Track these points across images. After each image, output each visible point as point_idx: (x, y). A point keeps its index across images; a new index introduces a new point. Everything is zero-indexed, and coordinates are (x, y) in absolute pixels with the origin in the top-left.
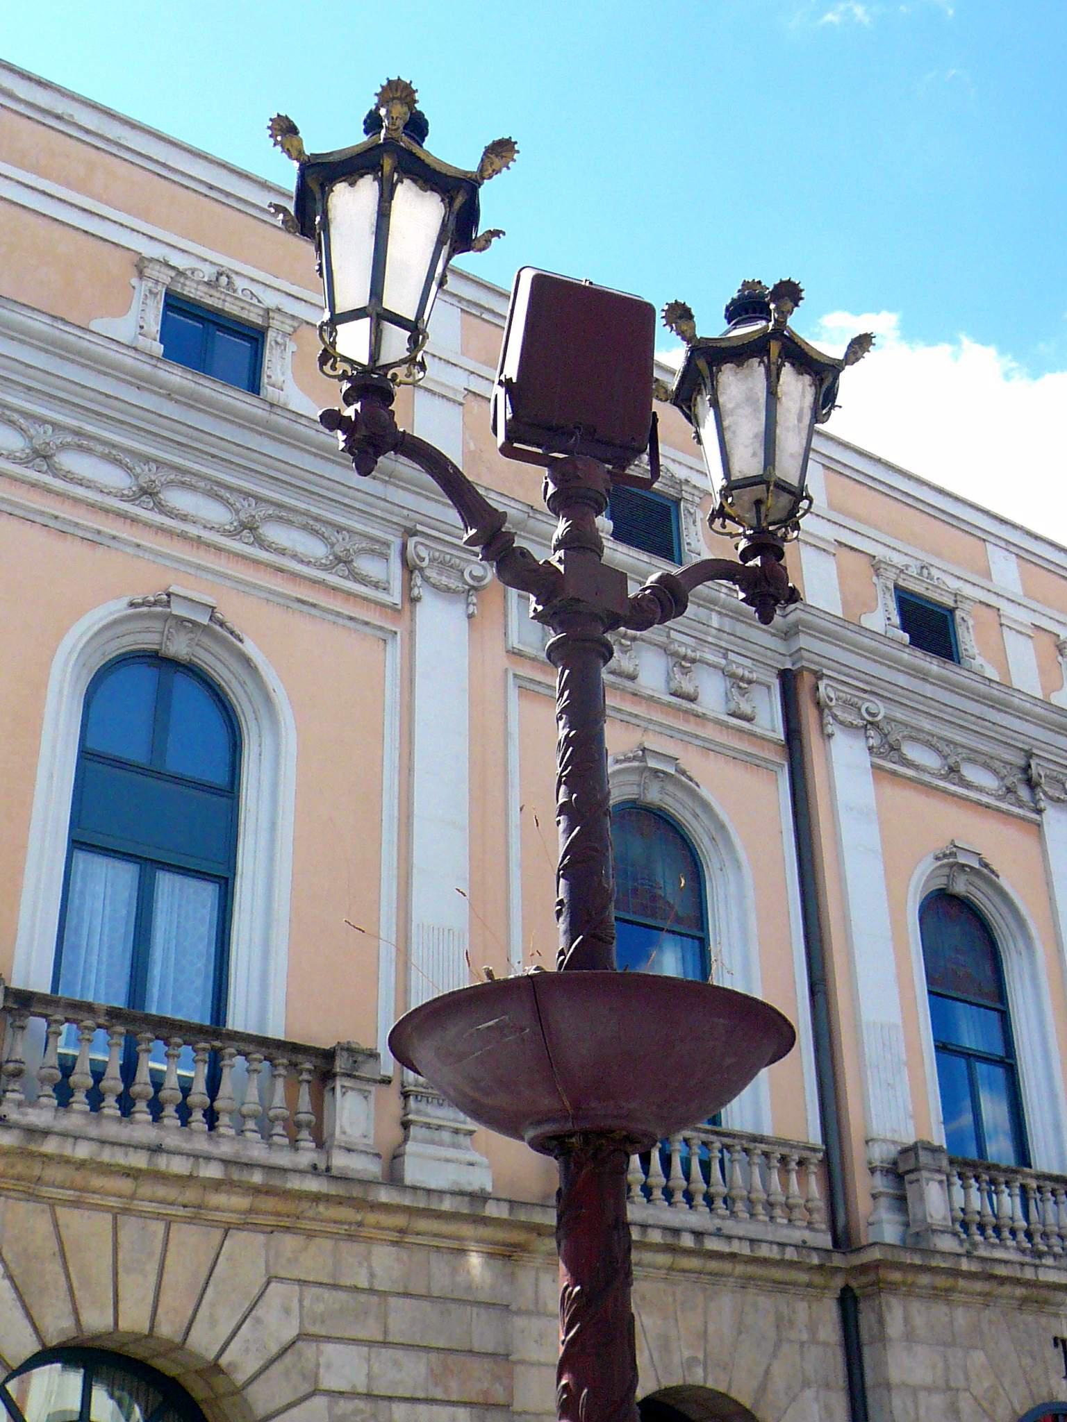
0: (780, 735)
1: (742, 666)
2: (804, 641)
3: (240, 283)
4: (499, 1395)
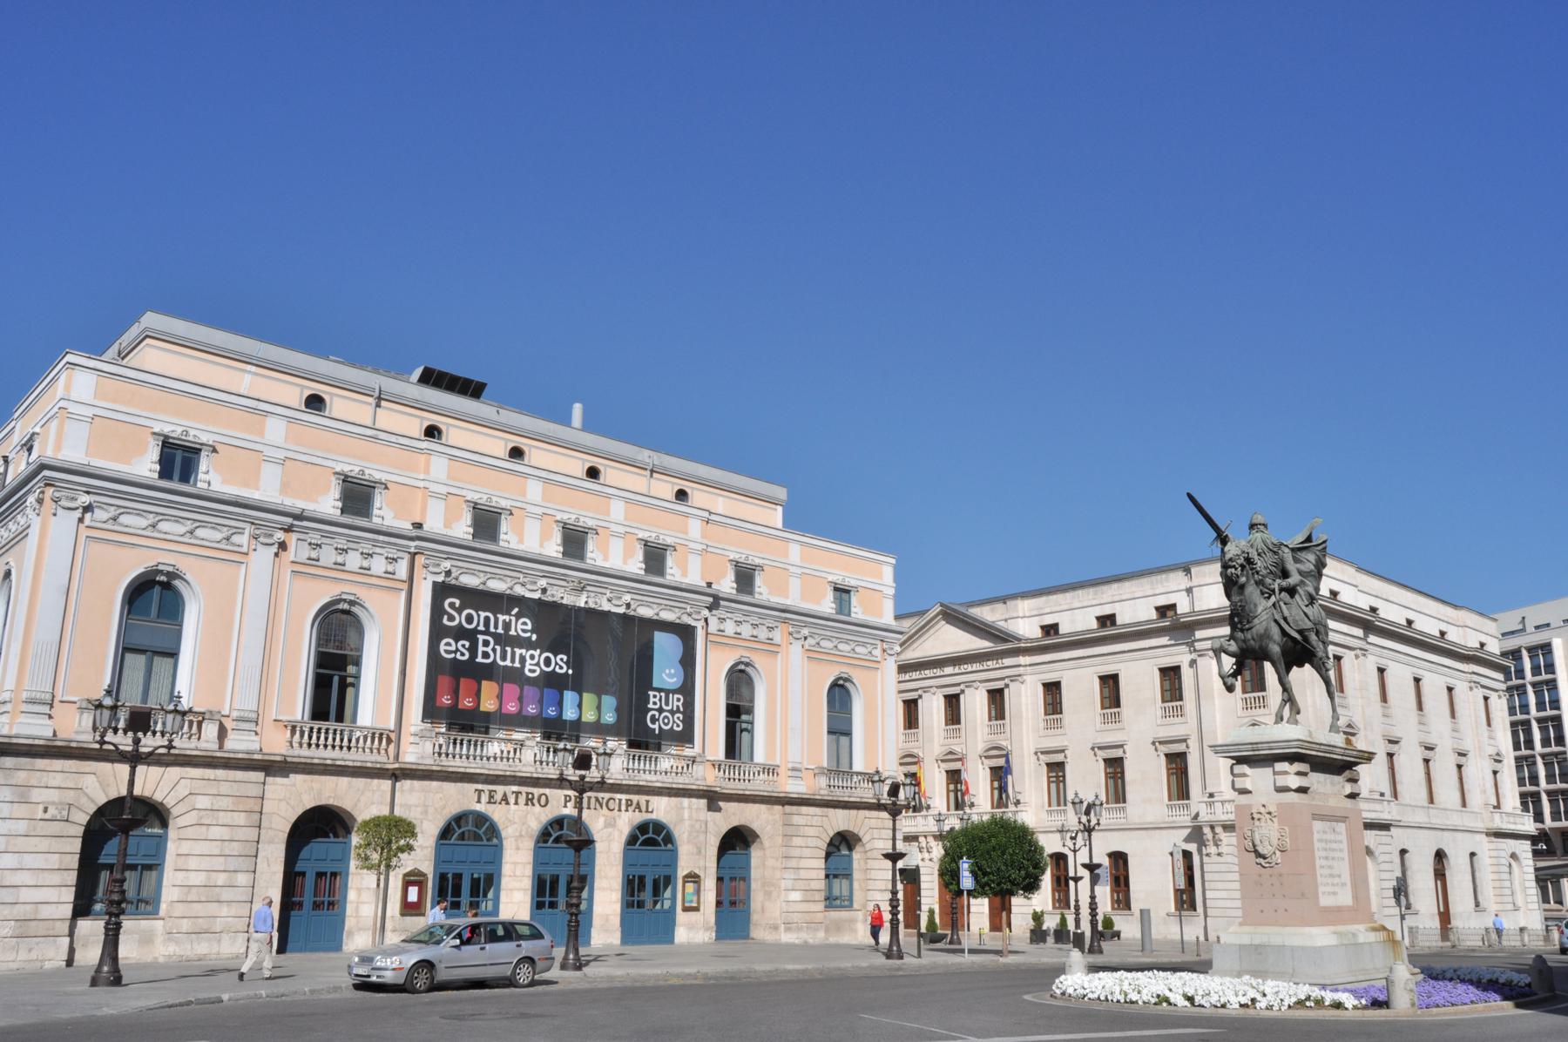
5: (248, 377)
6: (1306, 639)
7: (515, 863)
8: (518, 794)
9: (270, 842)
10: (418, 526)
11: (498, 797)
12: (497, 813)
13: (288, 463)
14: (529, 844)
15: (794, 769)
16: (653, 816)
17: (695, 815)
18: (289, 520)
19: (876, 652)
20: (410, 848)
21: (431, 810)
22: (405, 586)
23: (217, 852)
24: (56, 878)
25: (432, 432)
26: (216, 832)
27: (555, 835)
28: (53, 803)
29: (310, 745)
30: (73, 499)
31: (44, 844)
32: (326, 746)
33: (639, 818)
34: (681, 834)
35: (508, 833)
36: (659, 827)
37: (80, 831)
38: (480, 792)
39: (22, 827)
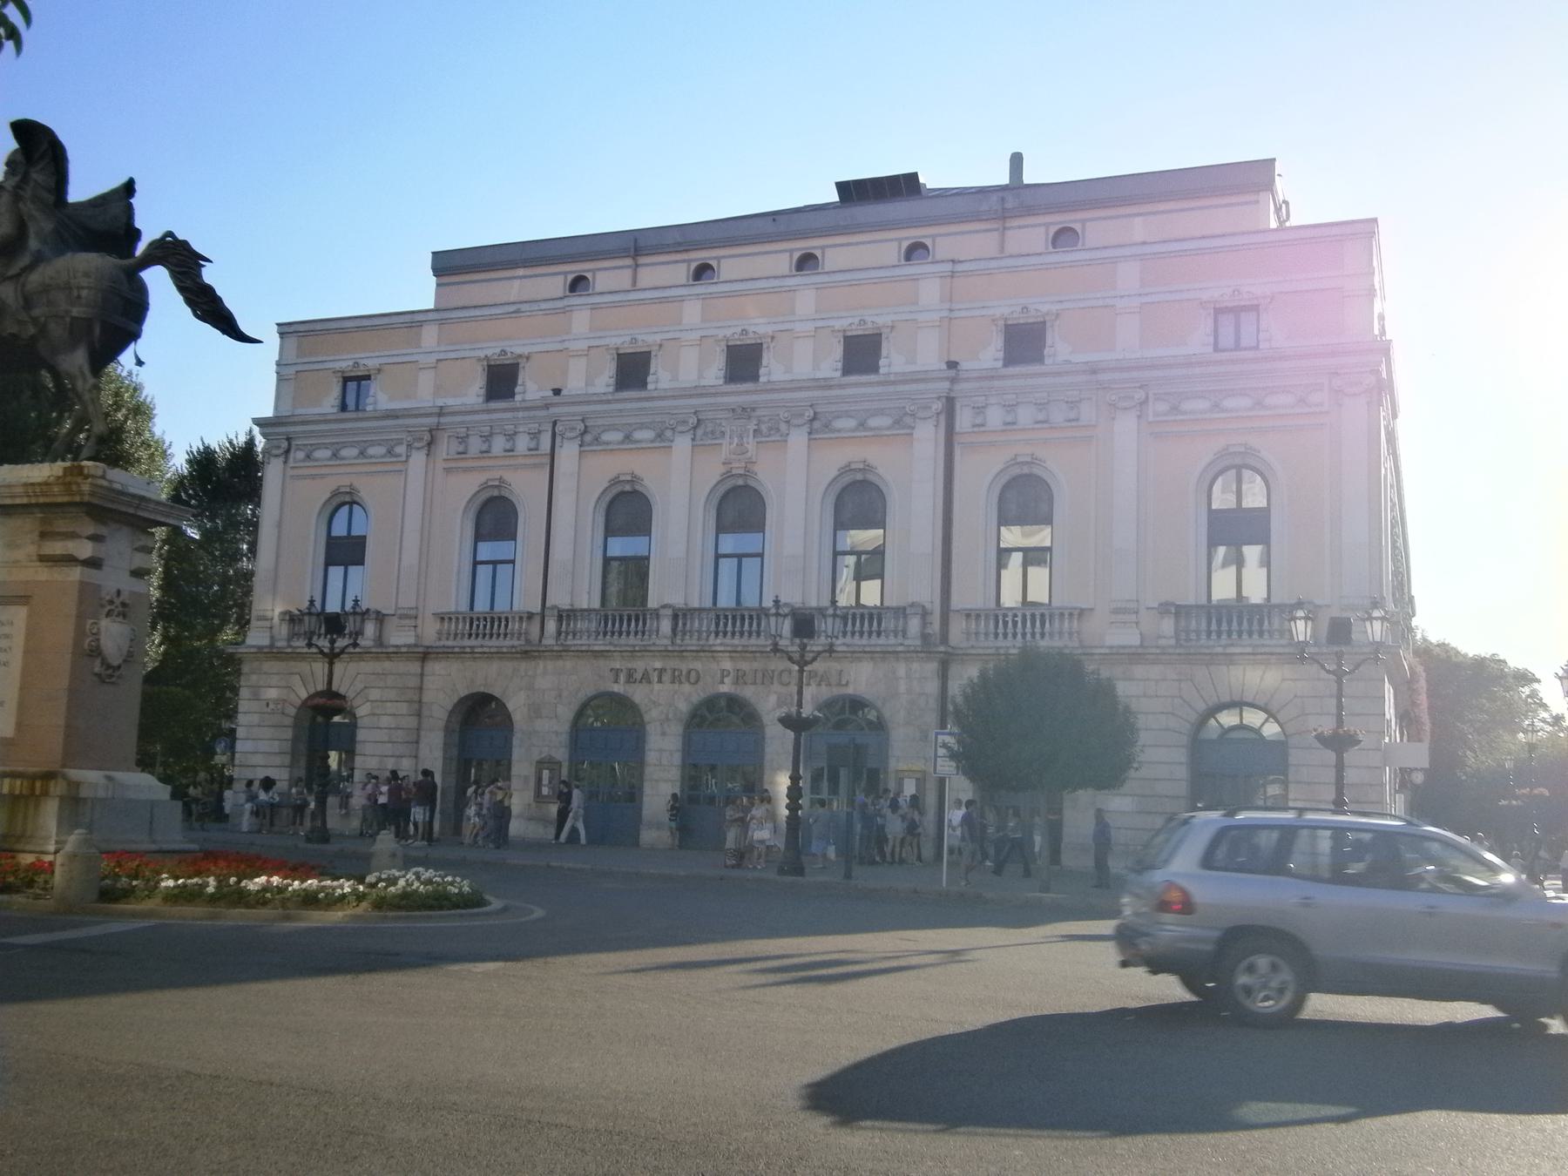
1: (534, 427)
5: (517, 283)
7: (661, 751)
8: (661, 671)
10: (557, 392)
11: (638, 676)
12: (638, 694)
14: (676, 729)
15: (1116, 611)
16: (850, 690)
22: (547, 460)
24: (277, 760)
25: (806, 262)
26: (385, 721)
29: (996, 635)
32: (733, 634)
35: (652, 715)
36: (857, 704)
38: (617, 672)
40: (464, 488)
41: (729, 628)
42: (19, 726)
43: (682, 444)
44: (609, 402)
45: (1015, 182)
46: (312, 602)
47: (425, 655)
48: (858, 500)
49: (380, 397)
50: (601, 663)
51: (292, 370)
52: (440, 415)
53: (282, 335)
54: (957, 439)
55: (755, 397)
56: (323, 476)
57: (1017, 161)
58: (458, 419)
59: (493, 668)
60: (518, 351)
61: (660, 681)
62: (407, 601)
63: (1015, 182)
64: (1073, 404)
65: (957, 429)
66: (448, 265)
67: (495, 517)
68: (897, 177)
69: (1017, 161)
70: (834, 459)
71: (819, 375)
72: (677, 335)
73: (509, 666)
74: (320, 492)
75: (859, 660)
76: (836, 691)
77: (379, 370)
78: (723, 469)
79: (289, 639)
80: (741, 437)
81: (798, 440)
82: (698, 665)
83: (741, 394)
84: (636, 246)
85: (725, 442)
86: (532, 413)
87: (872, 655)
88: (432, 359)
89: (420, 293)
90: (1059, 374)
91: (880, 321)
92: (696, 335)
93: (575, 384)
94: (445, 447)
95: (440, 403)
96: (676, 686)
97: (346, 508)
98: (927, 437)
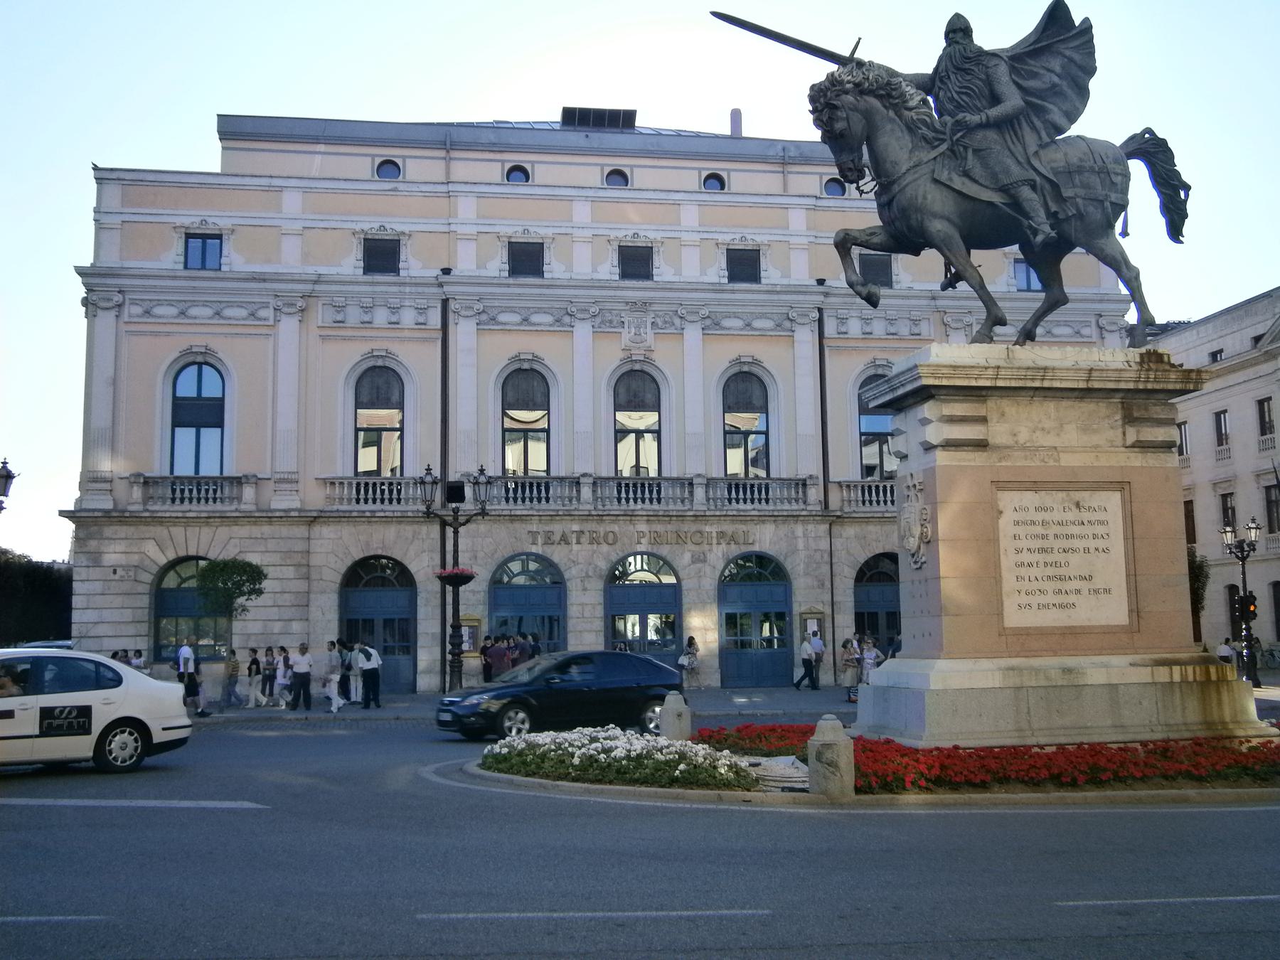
0: (439, 326)
1: (422, 303)
2: (446, 288)
3: (210, 220)
4: (304, 562)
5: (318, 158)
6: (1016, 204)
7: (582, 604)
9: (323, 592)
10: (446, 271)
11: (557, 537)
12: (557, 555)
13: (306, 231)
16: (756, 548)
17: (813, 545)
18: (309, 287)
19: (1085, 331)
20: (259, 592)
21: (481, 555)
22: (439, 335)
23: (270, 603)
24: (131, 630)
27: (868, 574)
28: (121, 566)
30: (109, 300)
31: (118, 601)
33: (735, 550)
34: (796, 567)
35: (572, 575)
36: (762, 560)
37: (146, 588)
38: (533, 534)
39: (98, 587)
40: (346, 358)
41: (647, 495)
42: (1136, 611)
43: (583, 331)
44: (508, 286)
45: (736, 135)
46: (429, 470)
47: (314, 519)
48: (745, 389)
49: (235, 259)
50: (517, 525)
51: (117, 220)
52: (315, 282)
53: (99, 180)
54: (825, 342)
55: (652, 294)
56: (168, 334)
57: (736, 116)
58: (334, 288)
59: (391, 532)
60: (399, 228)
61: (578, 543)
62: (286, 464)
63: (736, 135)
64: (916, 322)
65: (826, 335)
66: (234, 130)
67: (379, 384)
68: (574, 109)
69: (736, 116)
70: (724, 354)
71: (706, 279)
72: (569, 231)
73: (408, 530)
74: (170, 350)
75: (763, 522)
76: (745, 549)
77: (233, 231)
78: (621, 355)
79: (145, 502)
80: (638, 327)
81: (693, 334)
82: (616, 528)
83: (635, 290)
84: (448, 139)
85: (625, 331)
86: (420, 289)
87: (774, 518)
88: (298, 226)
89: (205, 155)
90: (904, 297)
91: (759, 239)
92: (588, 233)
93: (465, 264)
94: (321, 315)
95: (311, 270)
96: (595, 546)
97: (194, 368)
98: (806, 338)
